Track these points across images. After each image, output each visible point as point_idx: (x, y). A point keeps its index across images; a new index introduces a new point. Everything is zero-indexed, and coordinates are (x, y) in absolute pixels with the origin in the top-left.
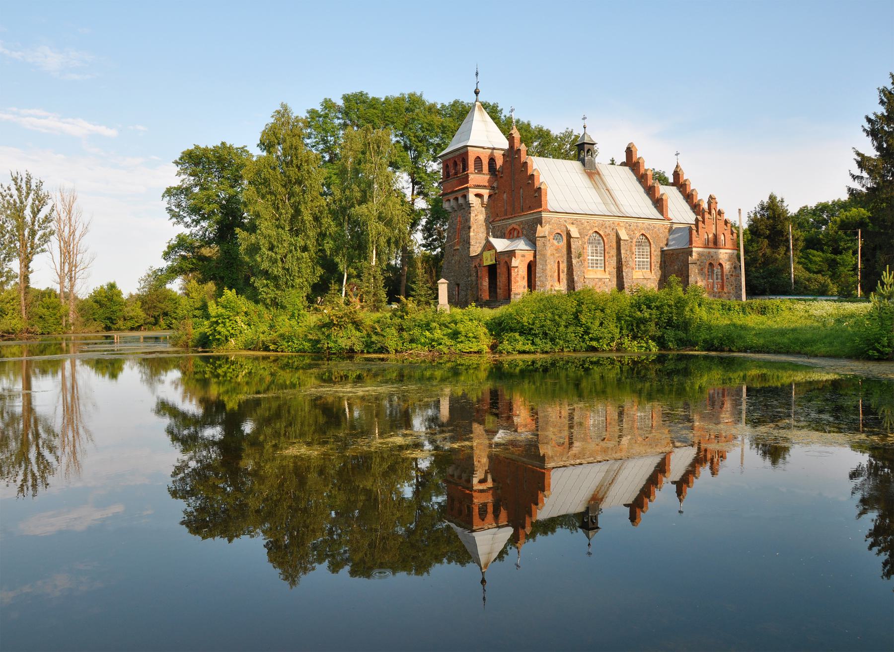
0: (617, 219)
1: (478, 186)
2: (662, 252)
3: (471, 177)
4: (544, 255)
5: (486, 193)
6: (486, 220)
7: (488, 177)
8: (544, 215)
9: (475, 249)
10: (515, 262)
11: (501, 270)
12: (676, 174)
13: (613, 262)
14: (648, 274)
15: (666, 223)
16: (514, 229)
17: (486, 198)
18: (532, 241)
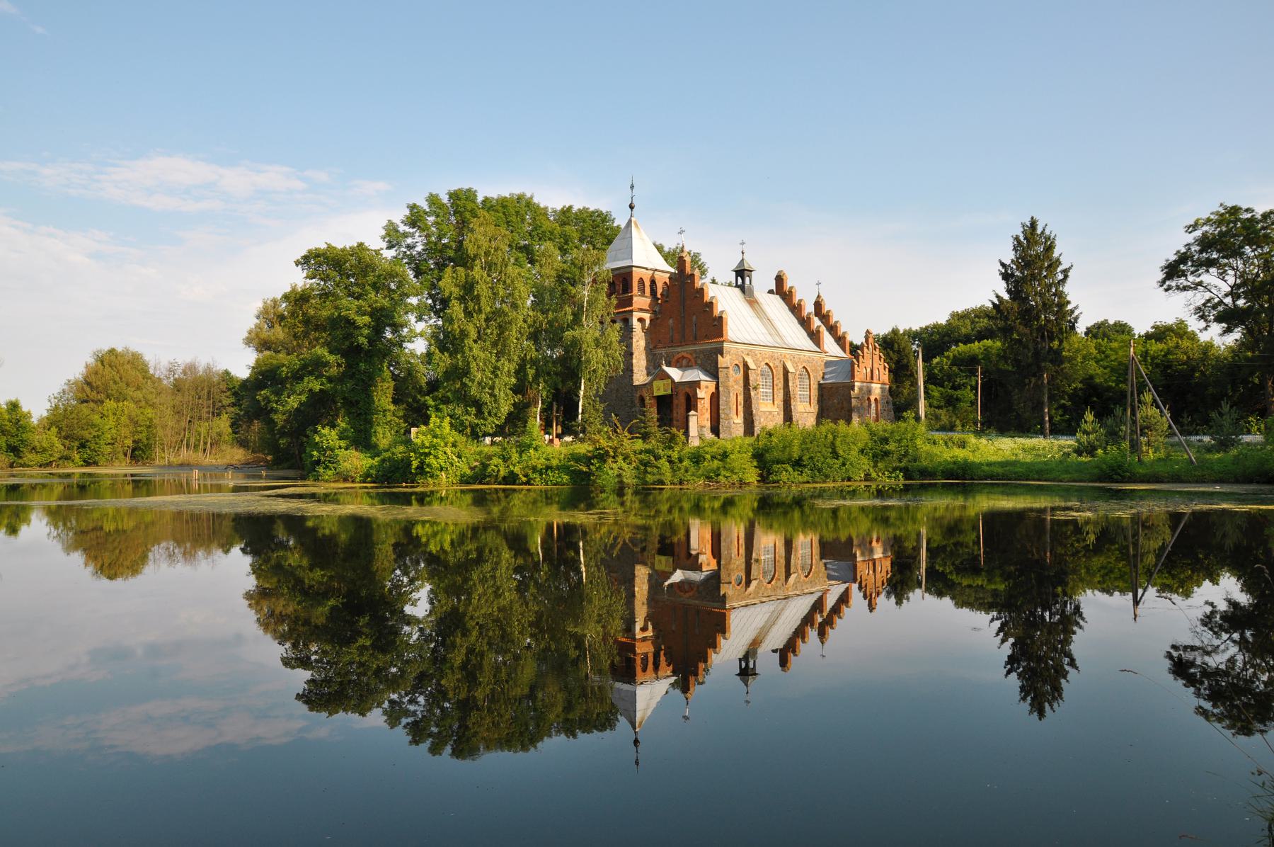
0: (784, 351)
1: (641, 310)
2: (820, 385)
3: (635, 299)
4: (727, 388)
5: (647, 316)
6: (646, 348)
7: (649, 300)
8: (725, 345)
9: (640, 377)
10: (700, 394)
11: (680, 402)
12: (818, 305)
13: (780, 395)
14: (809, 409)
15: (823, 355)
16: (683, 357)
17: (648, 322)
18: (714, 372)
